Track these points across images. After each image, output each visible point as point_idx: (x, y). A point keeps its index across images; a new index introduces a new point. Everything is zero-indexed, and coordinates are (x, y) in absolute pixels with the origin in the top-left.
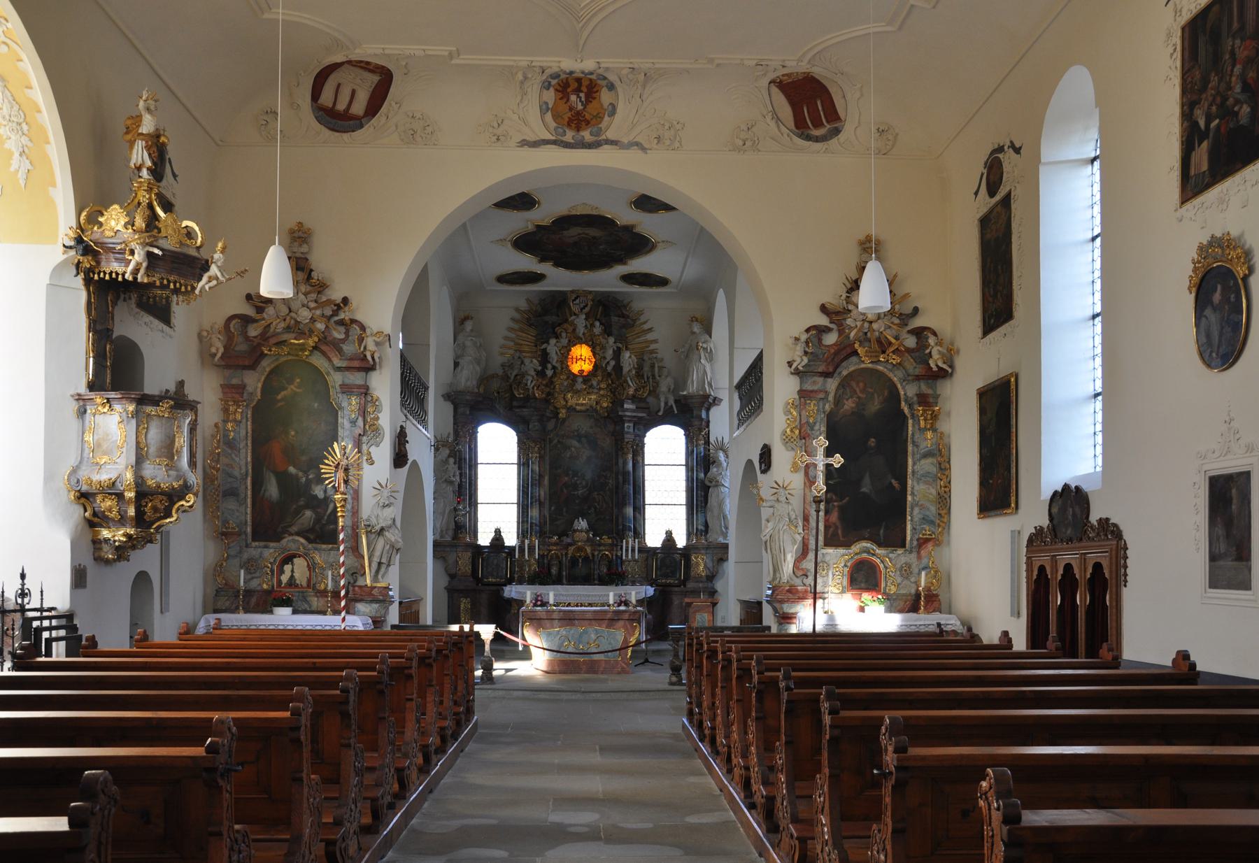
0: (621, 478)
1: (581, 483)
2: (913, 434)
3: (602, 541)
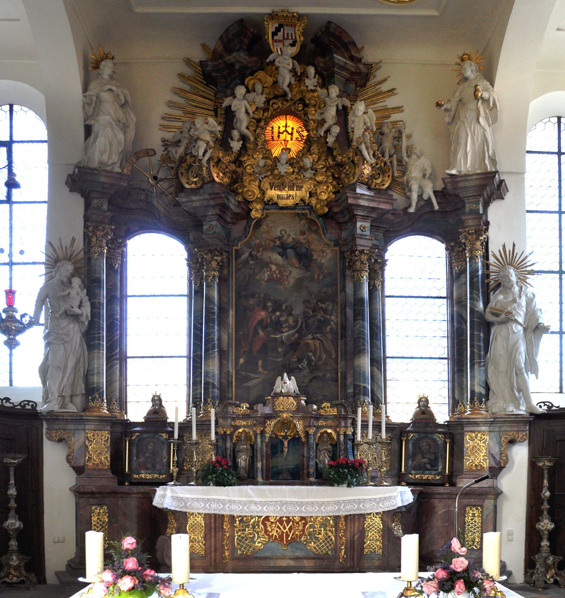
0: (350, 312)
1: (286, 321)
3: (322, 412)
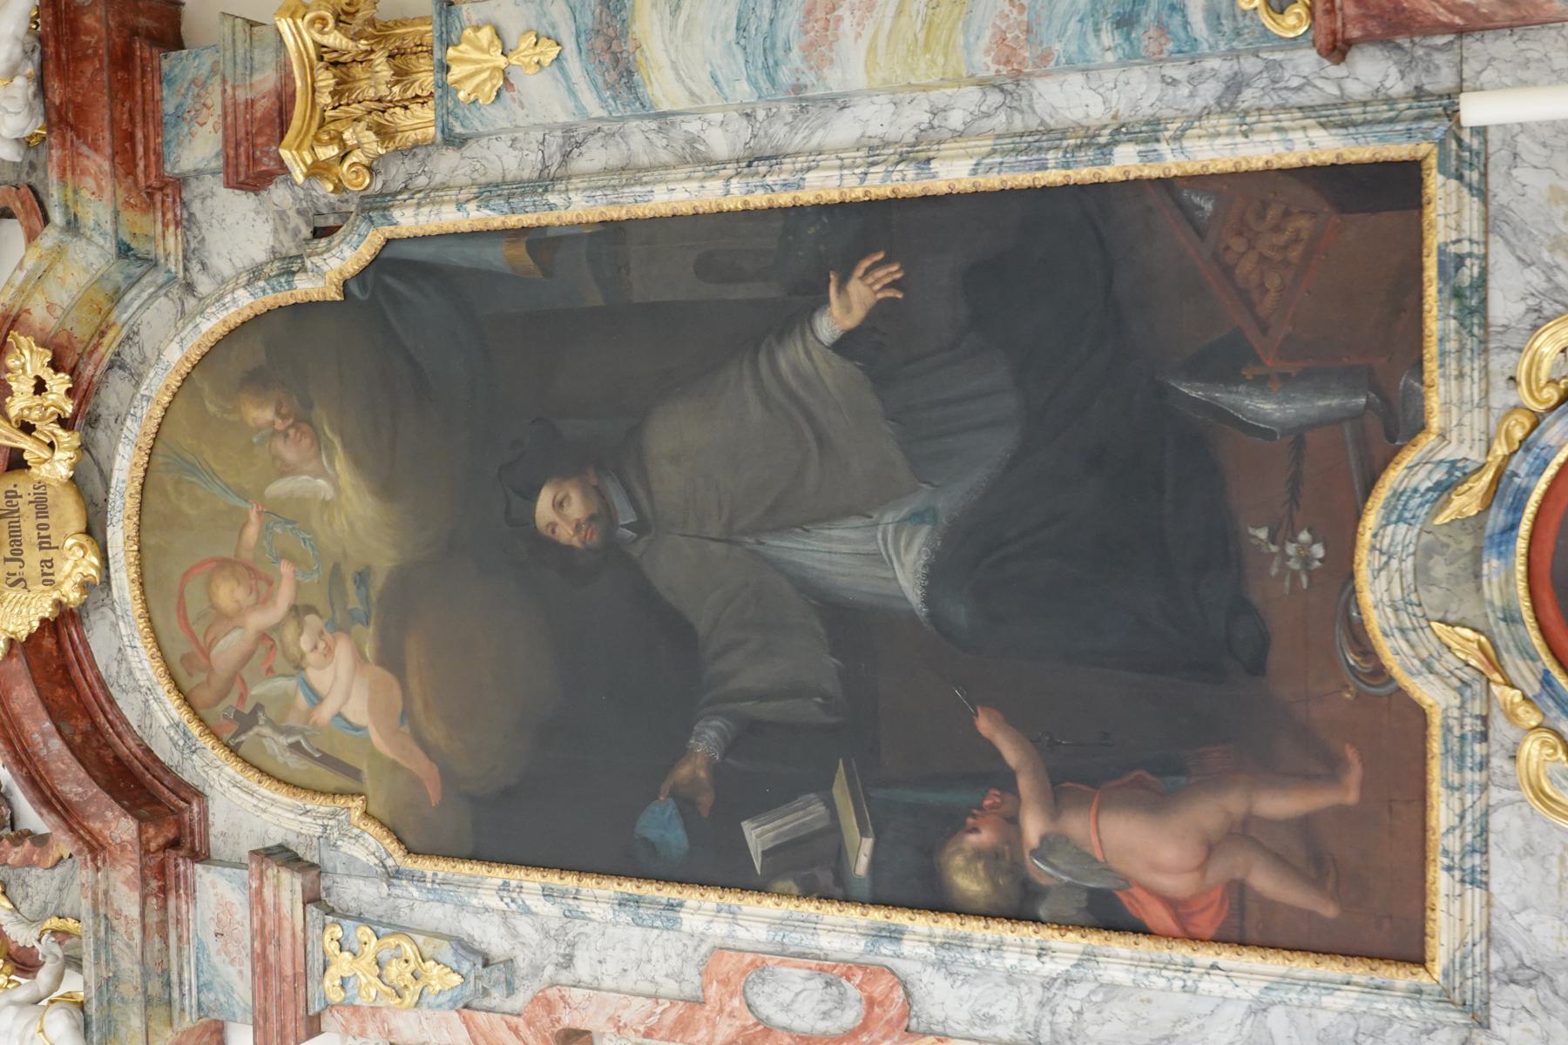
2: (487, 192)
